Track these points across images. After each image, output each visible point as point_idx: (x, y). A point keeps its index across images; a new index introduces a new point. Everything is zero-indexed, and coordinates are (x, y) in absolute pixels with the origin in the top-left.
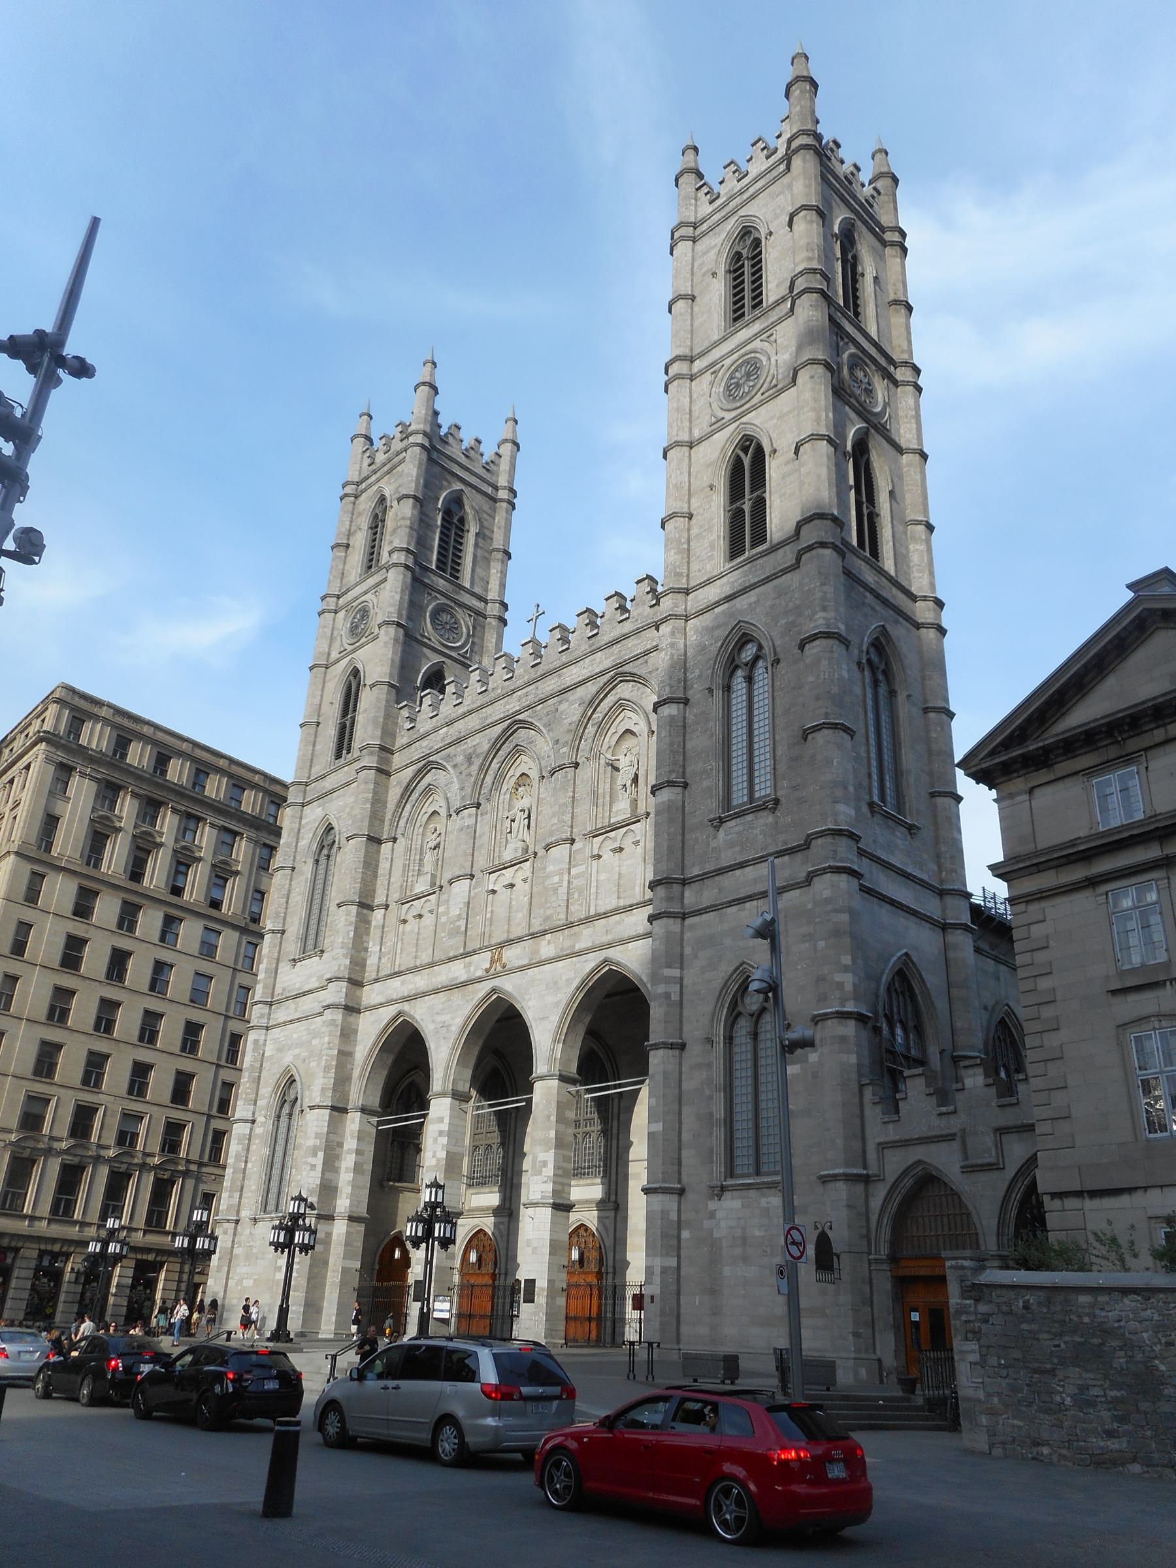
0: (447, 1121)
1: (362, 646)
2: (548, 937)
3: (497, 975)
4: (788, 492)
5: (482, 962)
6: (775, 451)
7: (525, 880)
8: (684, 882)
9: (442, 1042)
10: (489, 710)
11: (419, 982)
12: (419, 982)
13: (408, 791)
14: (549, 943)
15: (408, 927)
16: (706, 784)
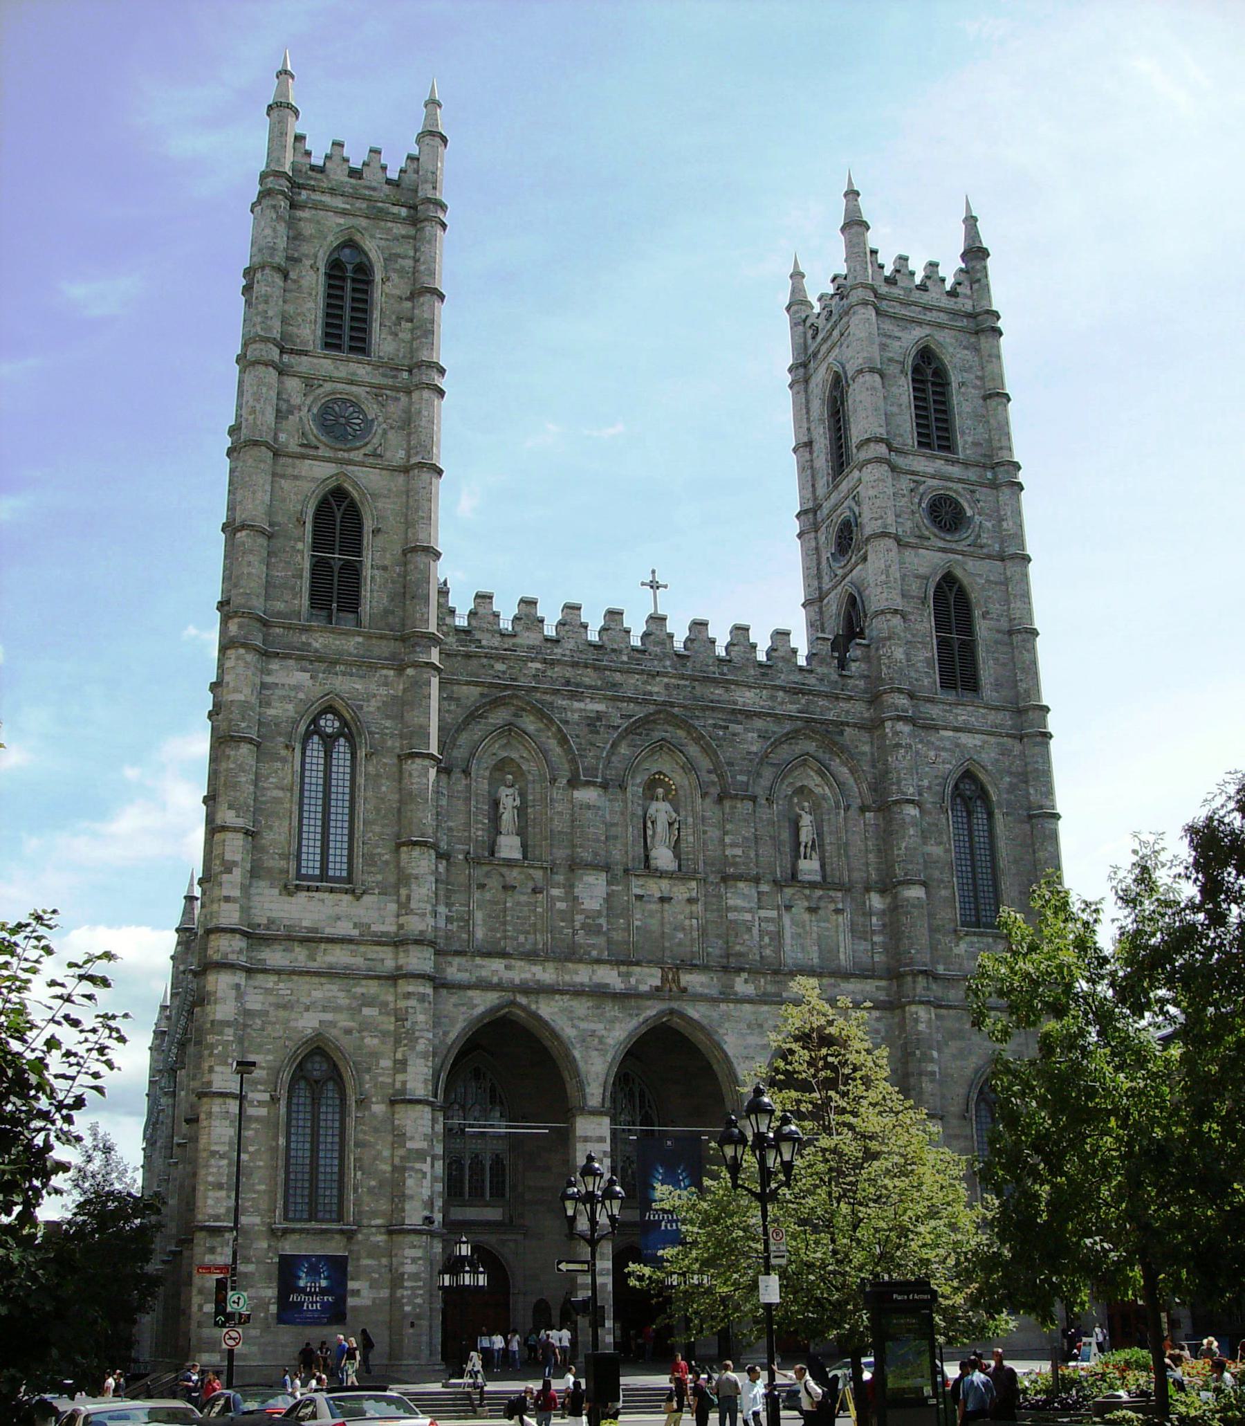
0: (608, 1141)
1: (362, 464)
2: (744, 975)
3: (677, 999)
4: (1001, 661)
5: (649, 978)
6: (988, 613)
7: (690, 901)
8: (936, 977)
9: (596, 1053)
10: (618, 677)
11: (545, 974)
12: (545, 974)
13: (473, 716)
14: (746, 981)
15: (488, 896)
16: (943, 893)
